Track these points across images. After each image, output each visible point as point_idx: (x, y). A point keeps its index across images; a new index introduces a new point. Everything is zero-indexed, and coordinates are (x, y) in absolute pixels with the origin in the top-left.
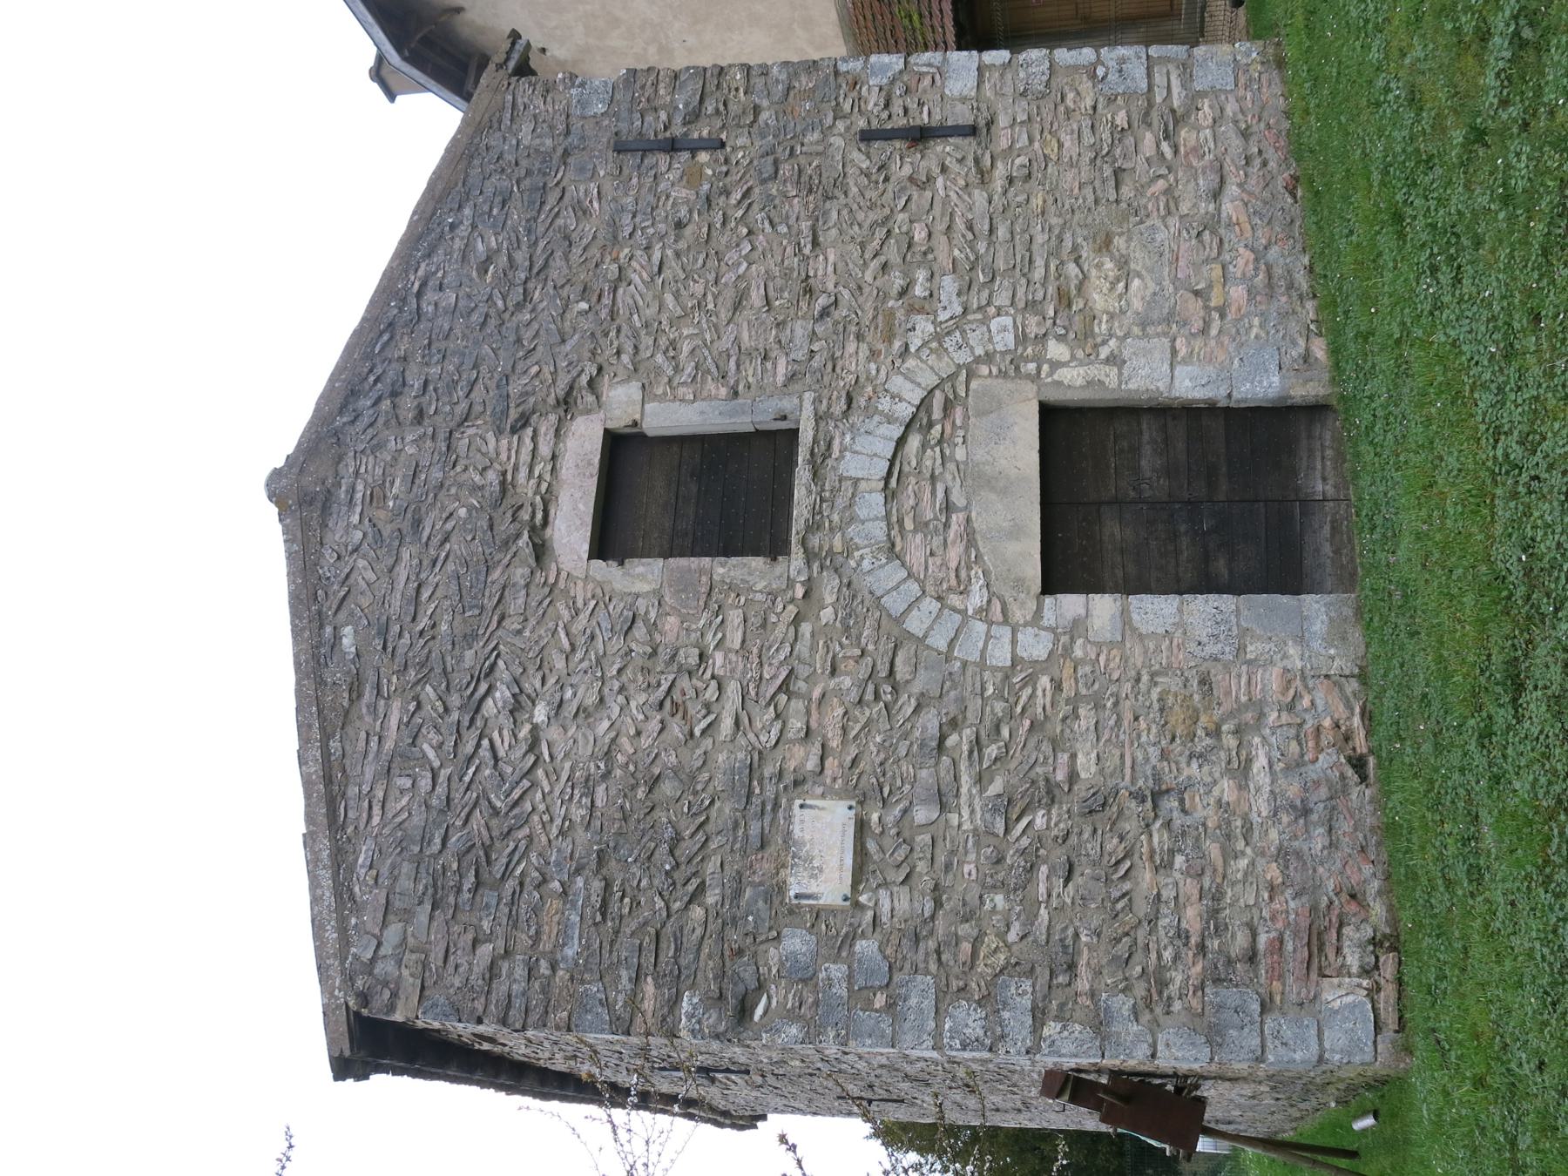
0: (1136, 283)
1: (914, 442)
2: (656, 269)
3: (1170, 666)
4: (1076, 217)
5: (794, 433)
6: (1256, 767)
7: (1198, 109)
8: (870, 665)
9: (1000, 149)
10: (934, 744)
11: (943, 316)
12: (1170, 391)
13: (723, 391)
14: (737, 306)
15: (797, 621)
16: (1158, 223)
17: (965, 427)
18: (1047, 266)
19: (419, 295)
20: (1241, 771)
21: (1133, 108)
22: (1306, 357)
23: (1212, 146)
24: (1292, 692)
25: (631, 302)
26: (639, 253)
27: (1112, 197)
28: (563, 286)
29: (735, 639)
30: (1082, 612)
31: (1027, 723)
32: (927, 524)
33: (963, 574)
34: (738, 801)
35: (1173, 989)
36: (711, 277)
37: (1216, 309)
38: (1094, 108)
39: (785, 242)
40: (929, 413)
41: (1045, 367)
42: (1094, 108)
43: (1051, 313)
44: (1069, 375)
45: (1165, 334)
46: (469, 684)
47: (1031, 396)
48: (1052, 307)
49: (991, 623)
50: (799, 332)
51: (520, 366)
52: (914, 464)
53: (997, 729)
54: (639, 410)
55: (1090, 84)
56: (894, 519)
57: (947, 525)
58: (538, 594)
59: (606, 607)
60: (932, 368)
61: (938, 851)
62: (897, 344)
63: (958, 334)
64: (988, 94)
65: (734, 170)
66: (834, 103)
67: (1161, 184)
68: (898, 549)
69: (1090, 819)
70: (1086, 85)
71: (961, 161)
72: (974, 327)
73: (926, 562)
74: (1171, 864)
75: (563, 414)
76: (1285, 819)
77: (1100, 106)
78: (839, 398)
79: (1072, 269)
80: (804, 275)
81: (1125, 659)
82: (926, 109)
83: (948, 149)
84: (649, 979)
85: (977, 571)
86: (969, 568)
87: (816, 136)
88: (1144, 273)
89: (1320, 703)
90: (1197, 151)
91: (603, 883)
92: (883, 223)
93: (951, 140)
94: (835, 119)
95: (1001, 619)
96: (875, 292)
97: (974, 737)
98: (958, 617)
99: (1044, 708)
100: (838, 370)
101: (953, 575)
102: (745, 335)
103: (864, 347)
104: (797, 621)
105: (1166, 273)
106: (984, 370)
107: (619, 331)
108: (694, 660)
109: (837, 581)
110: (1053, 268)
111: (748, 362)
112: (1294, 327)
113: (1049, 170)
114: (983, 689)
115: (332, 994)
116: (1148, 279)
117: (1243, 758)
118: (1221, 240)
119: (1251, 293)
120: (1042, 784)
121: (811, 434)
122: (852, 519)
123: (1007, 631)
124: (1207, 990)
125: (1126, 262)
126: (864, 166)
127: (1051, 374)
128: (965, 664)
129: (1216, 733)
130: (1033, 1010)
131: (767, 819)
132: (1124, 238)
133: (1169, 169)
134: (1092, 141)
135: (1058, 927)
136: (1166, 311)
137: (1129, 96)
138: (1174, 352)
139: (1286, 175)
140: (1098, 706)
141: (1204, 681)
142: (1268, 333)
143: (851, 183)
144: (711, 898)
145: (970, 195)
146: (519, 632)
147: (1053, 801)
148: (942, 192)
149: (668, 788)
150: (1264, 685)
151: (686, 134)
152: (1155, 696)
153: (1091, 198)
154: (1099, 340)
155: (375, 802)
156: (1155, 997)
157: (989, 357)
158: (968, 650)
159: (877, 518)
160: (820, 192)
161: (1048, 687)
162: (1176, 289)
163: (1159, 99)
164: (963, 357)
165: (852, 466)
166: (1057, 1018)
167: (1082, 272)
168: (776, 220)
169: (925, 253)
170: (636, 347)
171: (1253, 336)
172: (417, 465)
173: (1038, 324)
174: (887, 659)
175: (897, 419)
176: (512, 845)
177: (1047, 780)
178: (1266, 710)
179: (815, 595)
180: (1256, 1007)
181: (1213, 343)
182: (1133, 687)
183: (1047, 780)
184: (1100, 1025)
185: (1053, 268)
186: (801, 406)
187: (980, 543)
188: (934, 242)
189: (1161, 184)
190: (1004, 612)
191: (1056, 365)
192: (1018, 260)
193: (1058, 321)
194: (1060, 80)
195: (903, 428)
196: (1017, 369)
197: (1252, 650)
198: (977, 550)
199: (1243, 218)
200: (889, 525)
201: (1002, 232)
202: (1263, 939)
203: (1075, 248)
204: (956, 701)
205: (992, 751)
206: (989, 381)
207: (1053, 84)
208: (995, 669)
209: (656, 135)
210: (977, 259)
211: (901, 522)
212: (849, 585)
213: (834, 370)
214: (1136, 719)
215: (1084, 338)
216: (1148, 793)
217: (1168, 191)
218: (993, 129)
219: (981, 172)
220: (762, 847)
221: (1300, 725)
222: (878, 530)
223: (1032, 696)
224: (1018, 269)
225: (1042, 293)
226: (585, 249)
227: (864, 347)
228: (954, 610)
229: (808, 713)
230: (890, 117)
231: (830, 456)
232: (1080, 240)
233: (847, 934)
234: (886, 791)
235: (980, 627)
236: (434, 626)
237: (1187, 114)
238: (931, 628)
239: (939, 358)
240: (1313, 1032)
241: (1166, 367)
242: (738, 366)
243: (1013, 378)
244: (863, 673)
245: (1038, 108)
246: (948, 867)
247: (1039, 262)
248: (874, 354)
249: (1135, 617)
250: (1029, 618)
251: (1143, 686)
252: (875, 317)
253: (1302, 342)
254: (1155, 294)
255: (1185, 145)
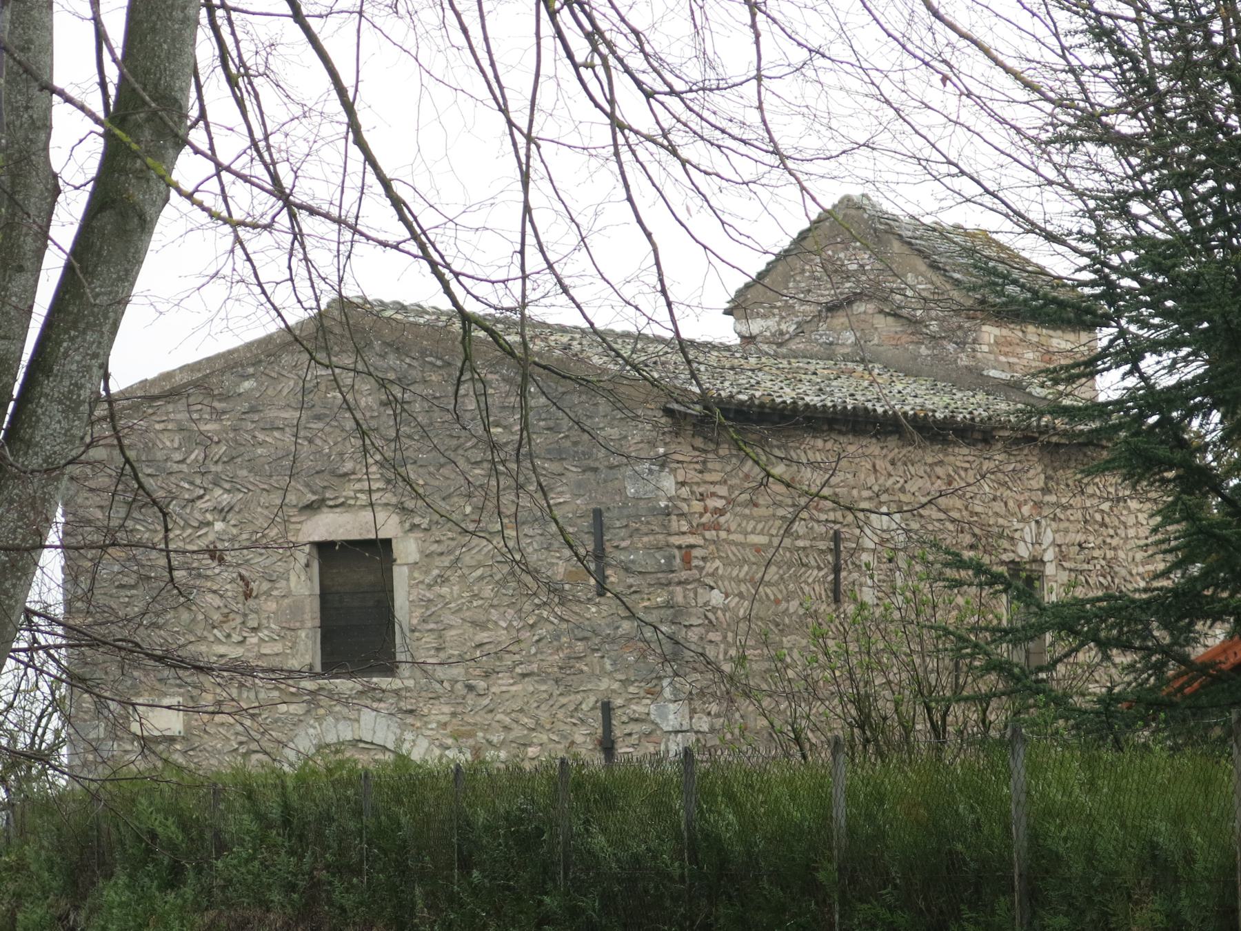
13: (415, 621)
14: (474, 624)
36: (495, 602)
62: (450, 741)
102: (453, 632)
107: (453, 539)
122: (337, 720)
126: (583, 706)
165: (367, 716)
168: (541, 644)
234: (191, 753)
242: (431, 630)
252: (469, 724)
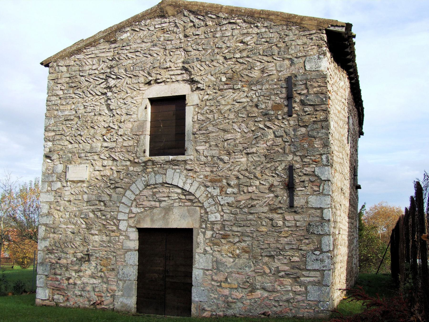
0: (232, 260)
1: (179, 191)
2: (238, 101)
3: (117, 261)
4: (256, 242)
5: (184, 154)
6: (94, 280)
7: (300, 286)
8: (118, 182)
9: (285, 216)
10: (100, 199)
11: (220, 198)
12: (195, 268)
13: (195, 130)
14: (224, 131)
15: (129, 160)
16: (252, 269)
17: (185, 206)
18: (238, 232)
19: (230, 23)
20: (92, 276)
21: (300, 263)
22: (204, 310)
23: (284, 290)
24: (110, 291)
25: (226, 95)
26: (245, 94)
27: (263, 254)
28: (232, 71)
29: (125, 144)
30: (131, 239)
31: (105, 223)
32: (155, 195)
33: (141, 206)
34: (89, 150)
35: (50, 256)
36: (235, 120)
37: (221, 284)
38: (301, 250)
39: (249, 143)
40: (188, 195)
41: (204, 230)
42: (301, 250)
43: (221, 232)
44: (201, 237)
45: (213, 268)
46: (114, 73)
47: (194, 226)
48: (223, 233)
49: (128, 214)
50: (214, 152)
51: (203, 64)
52: (172, 191)
53: (104, 216)
54: (190, 105)
55: (312, 248)
56: (156, 186)
57: (155, 201)
58: (136, 86)
59: (134, 106)
60: (202, 195)
61: (78, 201)
62: (209, 184)
63: (214, 203)
64: (309, 211)
65: (280, 122)
66: (306, 155)
67: (268, 271)
68: (148, 187)
69: (83, 238)
70: (312, 247)
71: (280, 202)
72: (216, 208)
73: (144, 196)
74: (75, 257)
75: (190, 80)
76: (82, 285)
77: (302, 252)
78: (192, 167)
79: (237, 240)
80: (236, 151)
81: (119, 249)
82: (304, 189)
83: (285, 197)
84: (55, 134)
85: (142, 210)
86: (143, 208)
87: (293, 149)
88: (234, 263)
89: (107, 298)
90: (281, 284)
91: (72, 119)
92: (255, 176)
93: (288, 199)
94: (300, 156)
95: (129, 217)
96: (228, 175)
97: (102, 209)
98: (130, 205)
99: (108, 228)
100: (202, 166)
101: (141, 203)
102: (214, 134)
103: (209, 173)
104: (129, 160)
105: (234, 270)
106: (203, 211)
107: (216, 93)
108: (119, 133)
109: (139, 171)
110: (237, 233)
111: (204, 137)
112: (215, 307)
113: (275, 233)
114: (113, 212)
115: (53, 58)
116: (232, 264)
117: (96, 277)
118: (247, 289)
119: (226, 296)
120: (91, 227)
121: (180, 159)
122: (156, 174)
123: (127, 218)
124: (50, 263)
125: (239, 258)
126: (279, 168)
127: (202, 232)
128: (118, 207)
129: (101, 271)
130: (47, 224)
131: (85, 158)
132: (247, 257)
133: (274, 274)
134: (287, 248)
135: (62, 230)
136: (221, 269)
137: (305, 263)
138: (208, 270)
139: (270, 313)
140: (109, 242)
141: (113, 269)
142: (212, 299)
143: (272, 164)
144: (70, 146)
145: (266, 206)
146: (127, 83)
147: (88, 229)
148: (267, 196)
149: (92, 131)
150: (112, 285)
151: (295, 102)
152: (110, 256)
153: (263, 247)
154: (212, 247)
155: (91, 55)
156: (49, 251)
157: (207, 213)
158: (122, 208)
159: (156, 181)
160: (268, 154)
161: (113, 229)
162: (228, 272)
163: (304, 273)
164: (206, 205)
165: (170, 172)
166: (46, 230)
167: (236, 243)
168: (258, 139)
169: (243, 191)
170: (210, 99)
171: (211, 294)
172: (172, 40)
173: (217, 228)
174: (119, 186)
175: (184, 185)
176: (80, 93)
177: (92, 228)
178: (107, 284)
179: (136, 164)
180: (46, 274)
181: (209, 282)
182: (112, 251)
183: (92, 228)
184: (44, 239)
185: (237, 233)
186: (188, 155)
187: (149, 211)
188: (247, 194)
189: (268, 271)
190: (131, 217)
191: (204, 233)
192: (239, 222)
193: (218, 234)
194: (315, 238)
195: (181, 187)
196: (203, 222)
197: (121, 283)
198: (148, 210)
199: (254, 297)
200: (153, 185)
201: (251, 217)
202: (59, 277)
203: (244, 241)
204: (110, 205)
205: (99, 214)
206: (199, 213)
207: (313, 235)
208: (117, 215)
209: (295, 91)
210: (241, 209)
211: (155, 188)
212: (138, 174)
213: (201, 164)
214: (106, 251)
215: (213, 242)
216: (88, 253)
217: (265, 273)
218: (293, 213)
219: (275, 209)
220: (79, 157)
221: (103, 292)
222: (152, 182)
223: (111, 225)
224: (237, 222)
225: (228, 230)
226: (247, 75)
227: (209, 173)
228: (132, 203)
229: (109, 166)
230: (300, 176)
231: (174, 166)
232: (248, 243)
233: (61, 180)
234: (90, 187)
235: (127, 211)
236: (129, 59)
237: (297, 282)
238: (127, 197)
239: (205, 197)
240: (42, 286)
241: (202, 267)
242: (203, 134)
243: (200, 220)
244: (117, 180)
245: (303, 230)
246: (74, 203)
247: (239, 229)
248: (206, 177)
249: (129, 253)
250: (130, 224)
251: (113, 253)
252: (219, 176)
253: (209, 309)
254: (226, 266)
255: (283, 280)
